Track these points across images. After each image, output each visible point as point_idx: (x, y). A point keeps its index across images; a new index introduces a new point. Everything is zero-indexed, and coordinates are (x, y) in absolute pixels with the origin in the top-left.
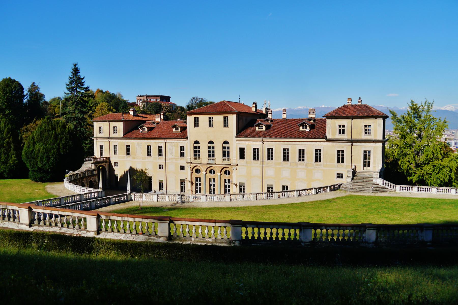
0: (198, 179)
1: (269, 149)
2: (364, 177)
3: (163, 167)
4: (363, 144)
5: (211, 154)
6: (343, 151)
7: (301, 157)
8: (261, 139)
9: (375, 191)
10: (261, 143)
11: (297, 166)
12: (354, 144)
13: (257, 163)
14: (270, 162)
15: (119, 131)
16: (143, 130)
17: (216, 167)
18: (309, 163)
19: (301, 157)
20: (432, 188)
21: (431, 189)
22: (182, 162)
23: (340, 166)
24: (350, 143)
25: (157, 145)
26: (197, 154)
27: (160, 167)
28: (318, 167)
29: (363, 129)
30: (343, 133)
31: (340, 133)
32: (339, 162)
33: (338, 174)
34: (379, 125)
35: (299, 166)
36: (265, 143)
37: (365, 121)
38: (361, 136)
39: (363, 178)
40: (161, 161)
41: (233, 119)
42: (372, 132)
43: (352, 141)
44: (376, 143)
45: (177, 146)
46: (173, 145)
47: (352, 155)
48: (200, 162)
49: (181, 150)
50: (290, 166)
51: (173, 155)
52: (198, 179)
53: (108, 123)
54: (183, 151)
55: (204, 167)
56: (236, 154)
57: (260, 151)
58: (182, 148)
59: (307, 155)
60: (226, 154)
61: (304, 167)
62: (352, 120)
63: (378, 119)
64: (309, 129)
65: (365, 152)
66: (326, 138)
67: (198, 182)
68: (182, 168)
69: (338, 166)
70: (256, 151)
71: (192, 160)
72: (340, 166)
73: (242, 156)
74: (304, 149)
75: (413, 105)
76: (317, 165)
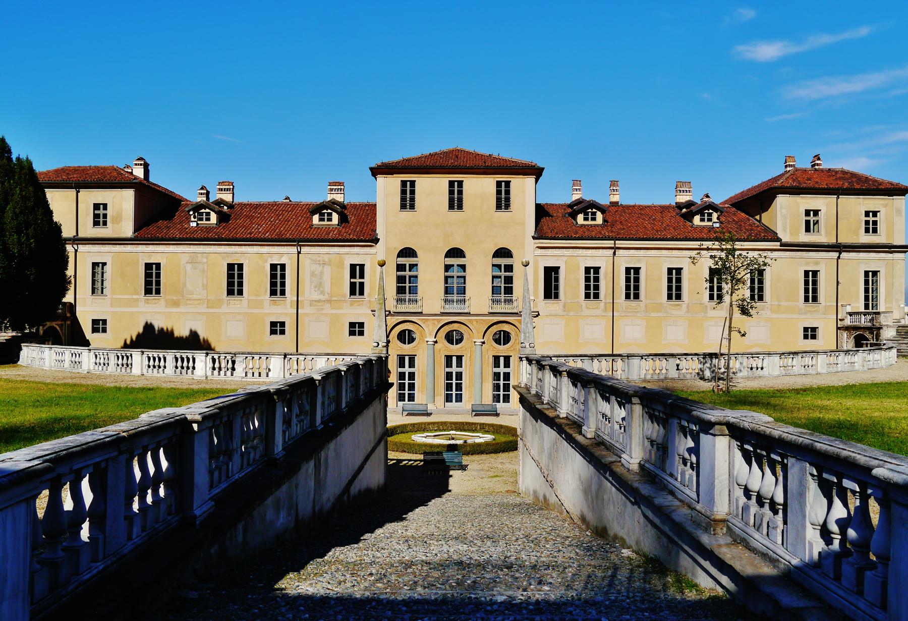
0: (407, 359)
1: (628, 270)
3: (287, 328)
6: (815, 273)
8: (613, 242)
10: (612, 251)
11: (706, 312)
12: (844, 255)
13: (597, 308)
14: (633, 303)
15: (118, 219)
17: (471, 321)
22: (359, 311)
25: (266, 261)
27: (277, 328)
31: (808, 229)
32: (806, 299)
33: (806, 329)
36: (618, 252)
37: (866, 202)
38: (858, 236)
40: (282, 310)
43: (839, 248)
44: (891, 252)
45: (341, 264)
46: (327, 260)
48: (420, 311)
49: (353, 275)
50: (688, 311)
51: (323, 293)
52: (407, 359)
53: (72, 192)
54: (358, 280)
55: (430, 323)
57: (606, 274)
58: (357, 270)
62: (838, 198)
63: (894, 197)
67: (407, 370)
70: (592, 275)
71: (391, 305)
73: (551, 290)
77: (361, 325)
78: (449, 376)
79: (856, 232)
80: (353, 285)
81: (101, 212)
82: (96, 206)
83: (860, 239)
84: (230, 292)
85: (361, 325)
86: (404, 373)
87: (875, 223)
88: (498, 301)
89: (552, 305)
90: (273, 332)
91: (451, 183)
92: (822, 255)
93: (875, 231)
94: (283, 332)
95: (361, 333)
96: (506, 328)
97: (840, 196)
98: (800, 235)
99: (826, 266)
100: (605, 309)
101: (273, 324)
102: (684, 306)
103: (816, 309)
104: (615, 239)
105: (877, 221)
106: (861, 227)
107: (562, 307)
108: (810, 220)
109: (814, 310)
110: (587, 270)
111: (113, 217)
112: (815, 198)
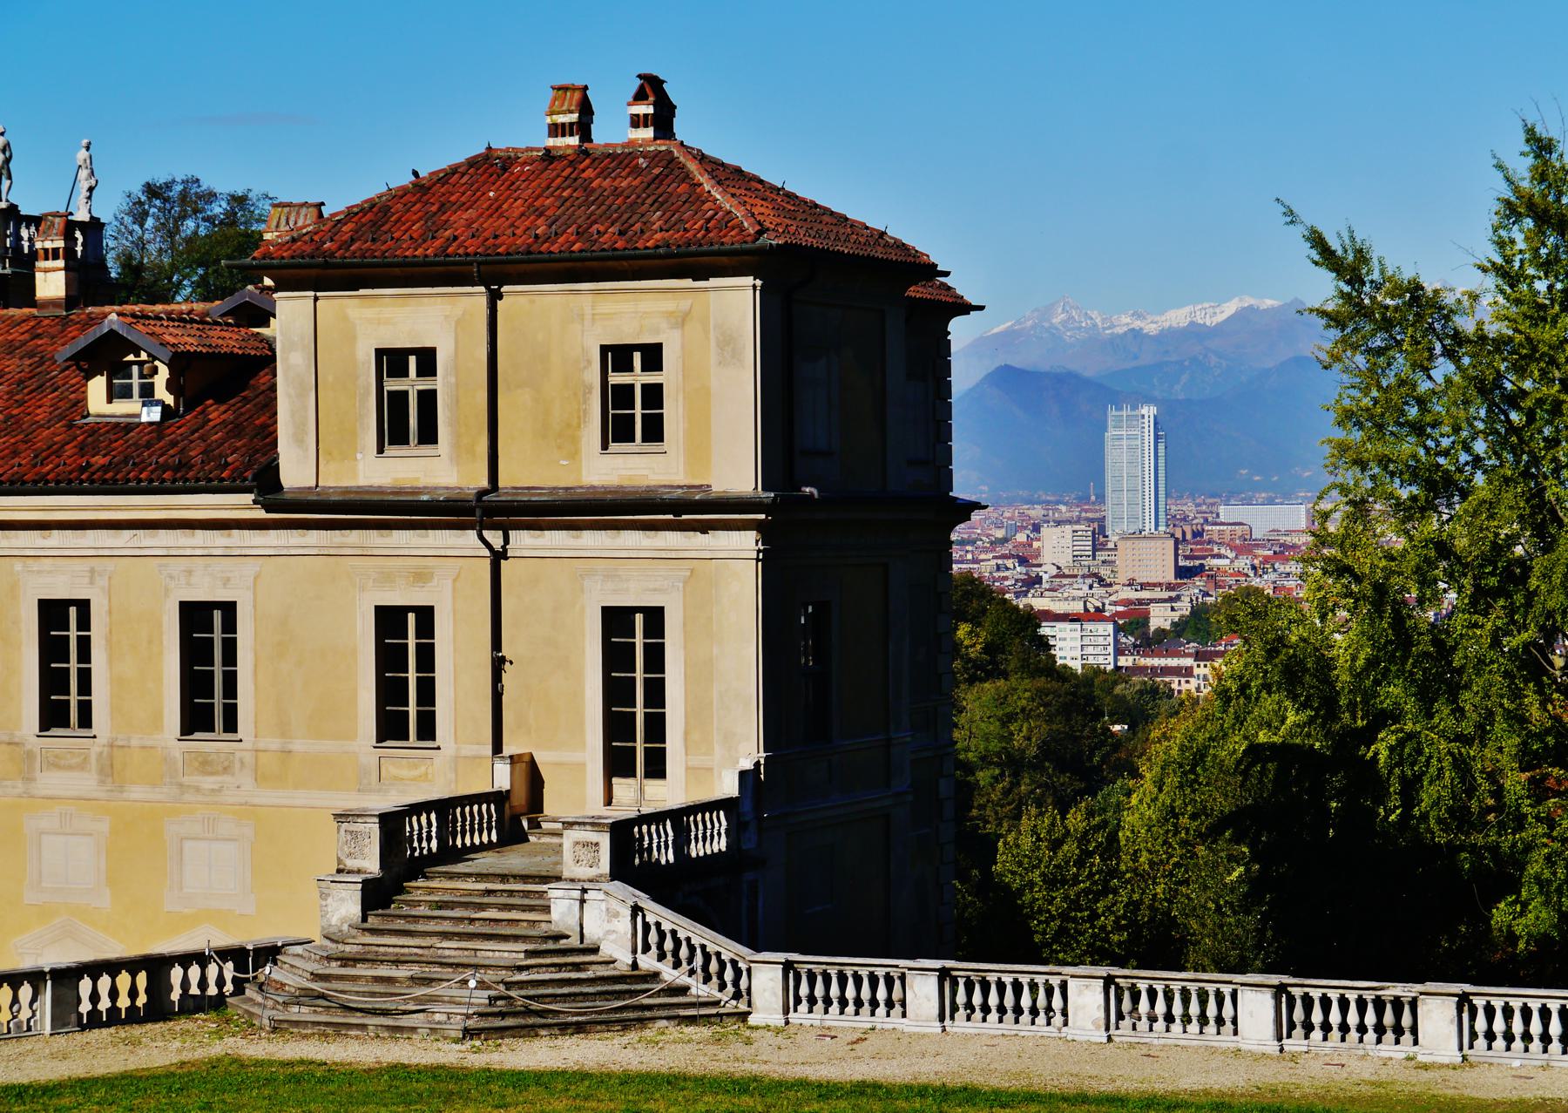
2: (504, 878)
9: (510, 1022)
11: (29, 779)
12: (522, 541)
18: (135, 742)
20: (1072, 985)
21: (1064, 987)
23: (405, 773)
24: (472, 534)
28: (208, 782)
29: (590, 389)
34: (727, 342)
35: (51, 782)
38: (574, 455)
39: (482, 886)
44: (704, 528)
47: (506, 651)
59: (110, 661)
61: (85, 783)
62: (494, 297)
64: (169, 400)
65: (616, 620)
66: (265, 482)
69: (390, 769)
72: (405, 773)
74: (234, 604)
75: (1541, 176)
76: (205, 765)
79: (568, 442)
83: (584, 473)
87: (654, 395)
92: (439, 543)
93: (654, 431)
97: (505, 289)
98: (359, 456)
99: (454, 589)
103: (423, 769)
105: (659, 387)
106: (583, 415)
108: (406, 393)
109: (415, 773)
112: (413, 301)
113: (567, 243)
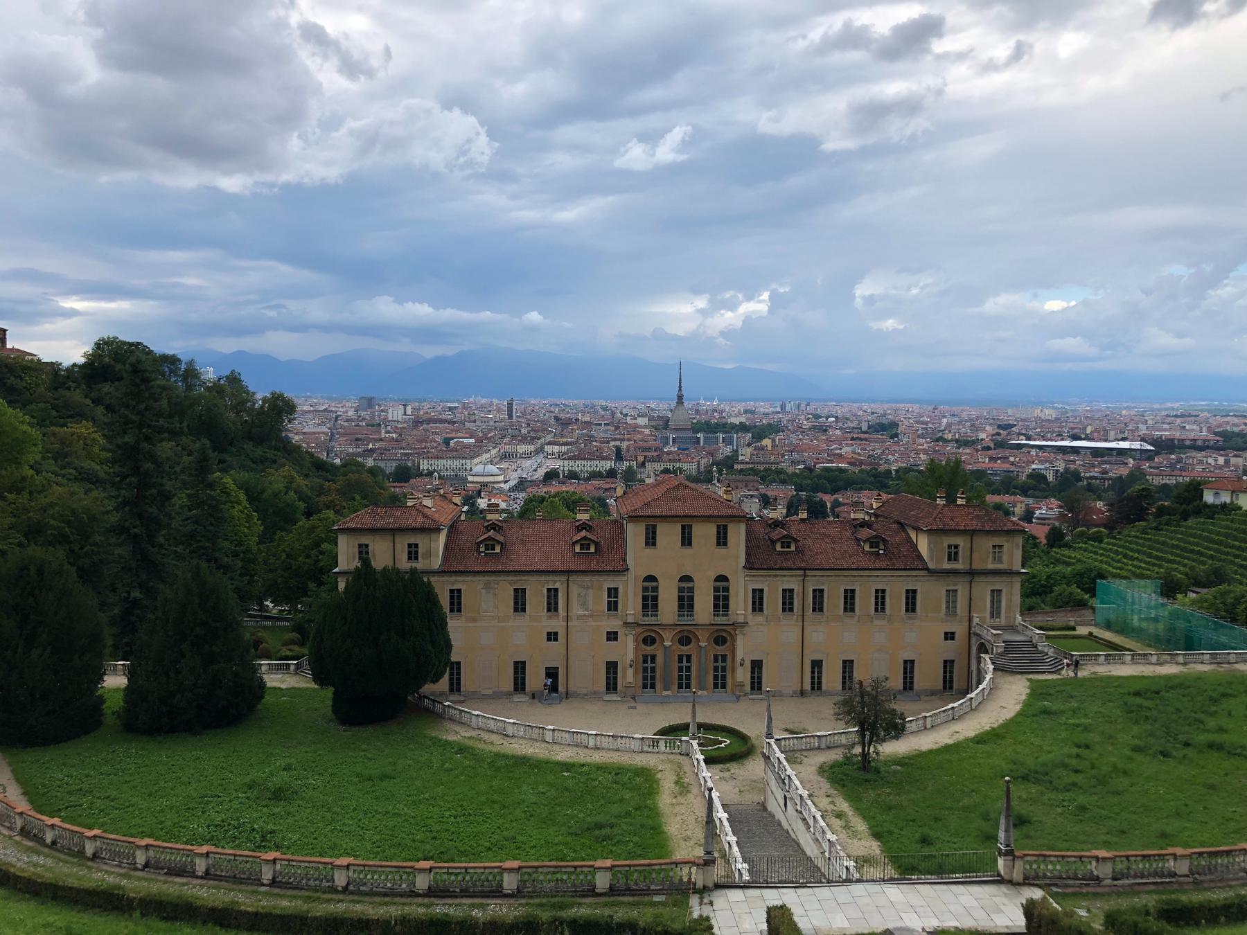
1: (814, 591)
4: (990, 579)
5: (686, 602)
7: (880, 605)
11: (872, 622)
14: (818, 616)
15: (428, 554)
16: (488, 550)
19: (880, 605)
22: (614, 624)
26: (650, 603)
27: (553, 636)
30: (956, 559)
31: (949, 559)
33: (946, 633)
34: (1017, 545)
35: (877, 622)
41: (738, 535)
42: (1005, 558)
49: (609, 596)
50: (859, 621)
56: (746, 601)
57: (798, 594)
58: (613, 592)
60: (721, 602)
61: (884, 622)
68: (612, 636)
70: (788, 594)
76: (910, 618)
77: (616, 633)
78: (680, 669)
80: (609, 602)
81: (413, 549)
82: (410, 546)
84: (516, 610)
85: (616, 633)
86: (647, 668)
88: (718, 615)
89: (759, 619)
90: (549, 639)
91: (683, 527)
94: (556, 639)
95: (616, 639)
96: (724, 634)
100: (797, 621)
101: (549, 634)
102: (856, 618)
104: (805, 569)
106: (988, 557)
107: (765, 619)
110: (784, 591)
111: (423, 554)
113: (987, 528)
